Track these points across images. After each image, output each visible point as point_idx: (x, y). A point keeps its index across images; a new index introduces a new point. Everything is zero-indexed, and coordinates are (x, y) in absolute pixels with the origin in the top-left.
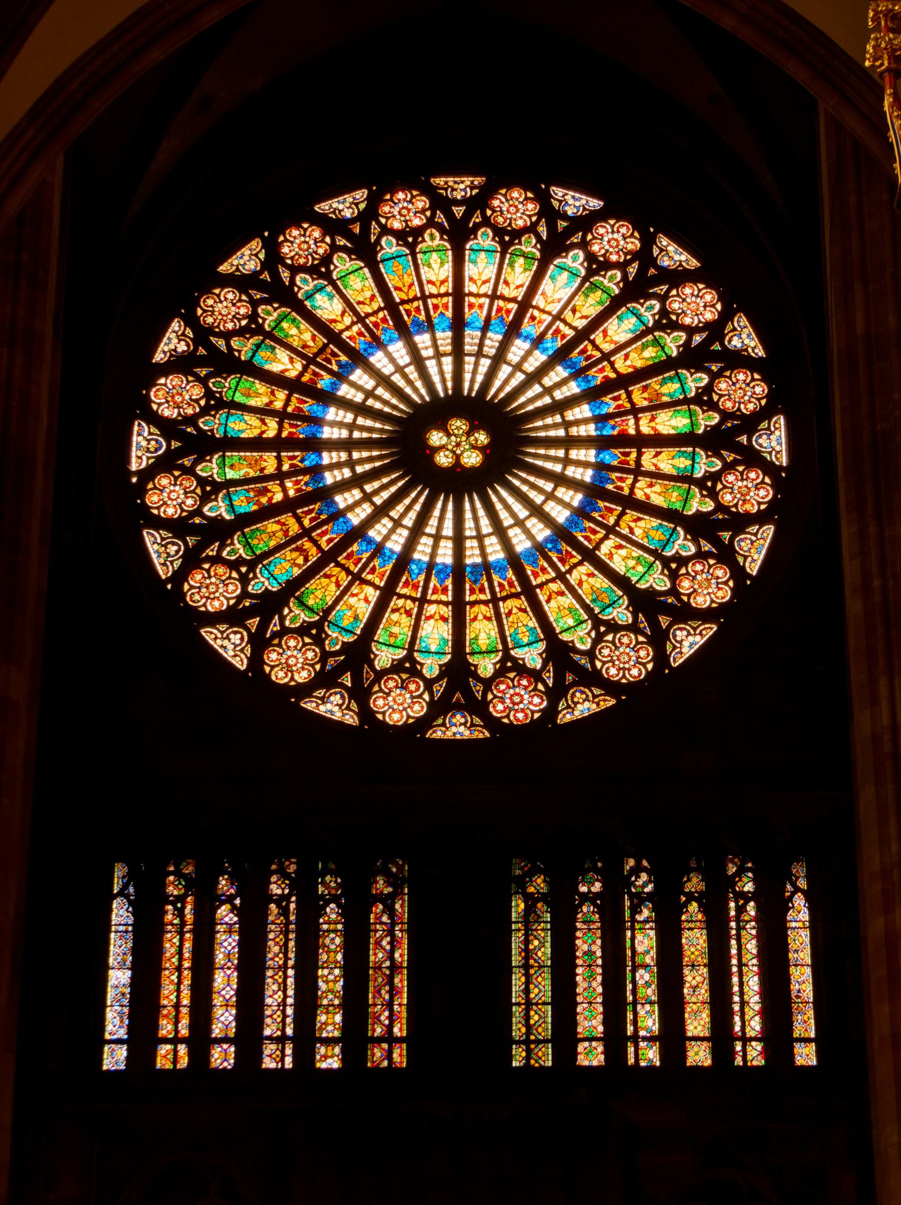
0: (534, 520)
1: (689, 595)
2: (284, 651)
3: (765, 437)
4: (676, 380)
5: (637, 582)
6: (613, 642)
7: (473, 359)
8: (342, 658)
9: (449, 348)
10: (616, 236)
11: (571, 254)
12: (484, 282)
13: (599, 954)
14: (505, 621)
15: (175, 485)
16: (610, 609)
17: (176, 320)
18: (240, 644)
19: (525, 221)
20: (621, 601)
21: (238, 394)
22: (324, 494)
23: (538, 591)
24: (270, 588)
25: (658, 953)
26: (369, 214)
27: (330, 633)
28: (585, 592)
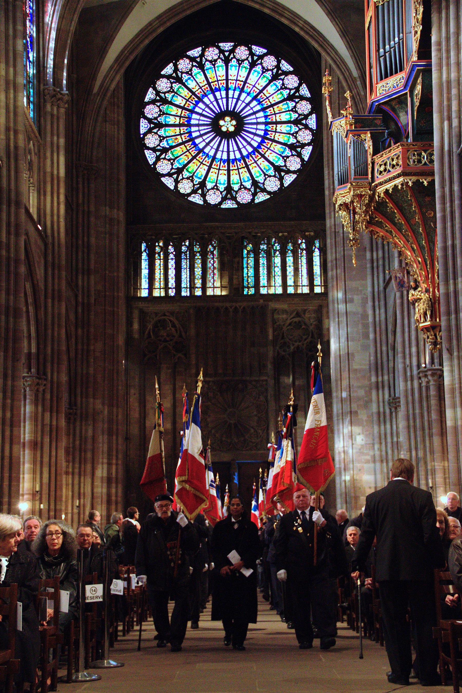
13: (266, 263)
22: (192, 140)
26: (202, 55)
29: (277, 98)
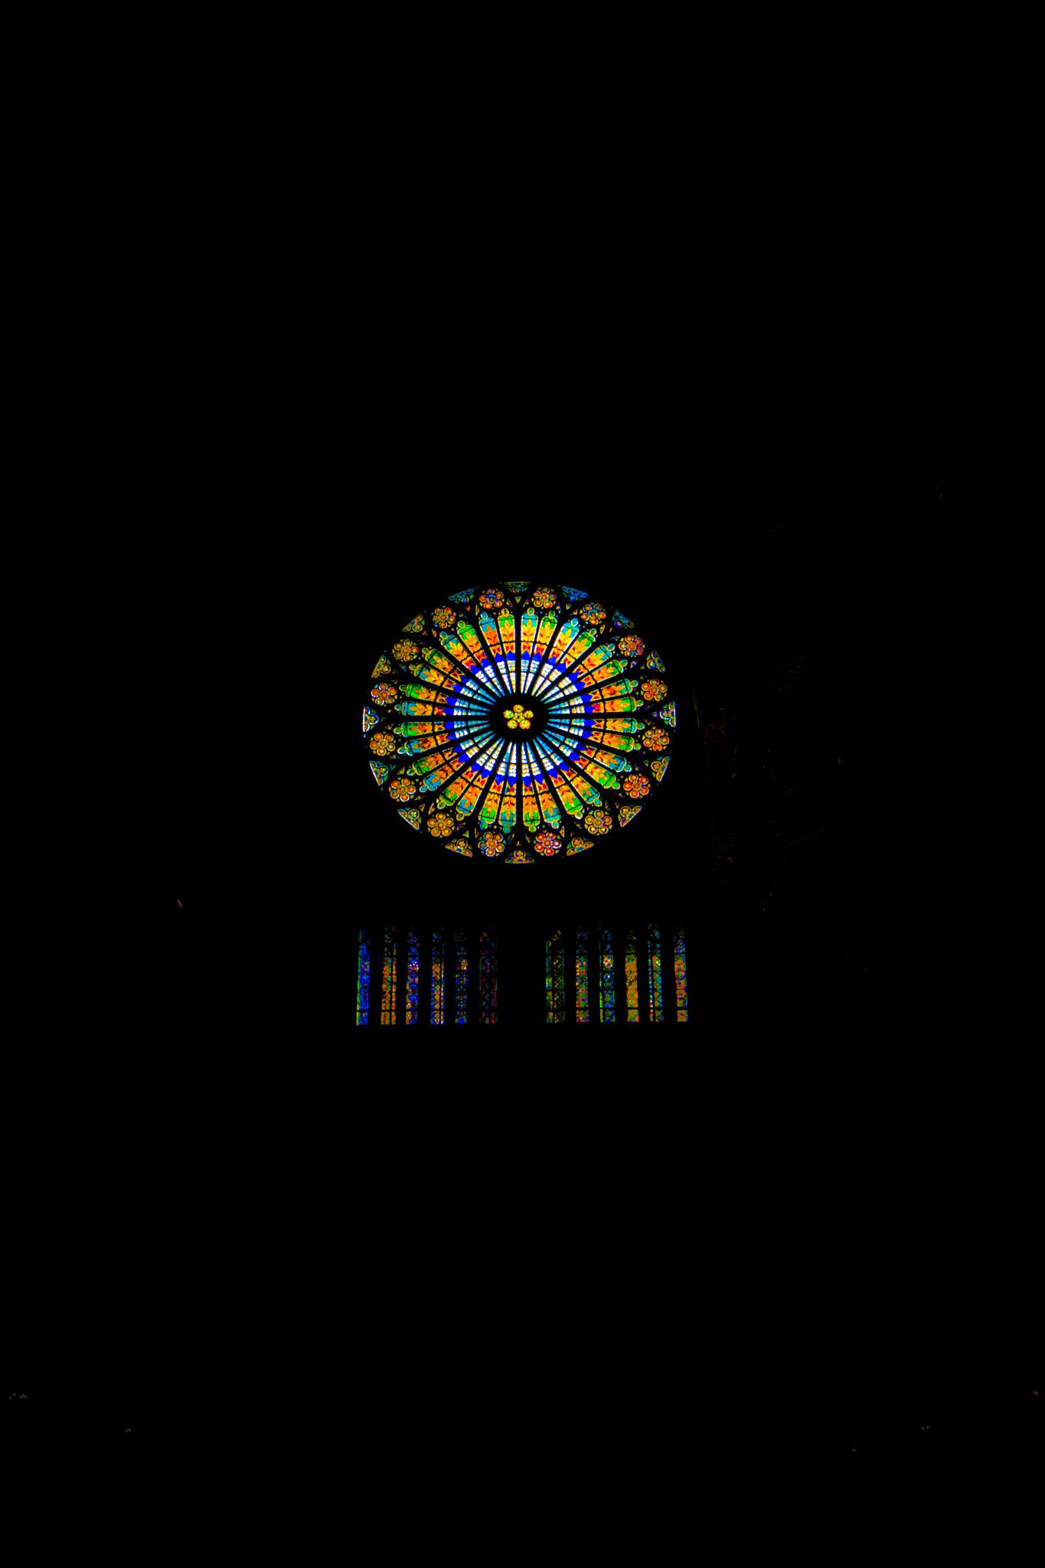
1: (629, 792)
6: (593, 815)
12: (531, 635)
22: (455, 744)
23: (557, 790)
26: (475, 602)
29: (609, 672)
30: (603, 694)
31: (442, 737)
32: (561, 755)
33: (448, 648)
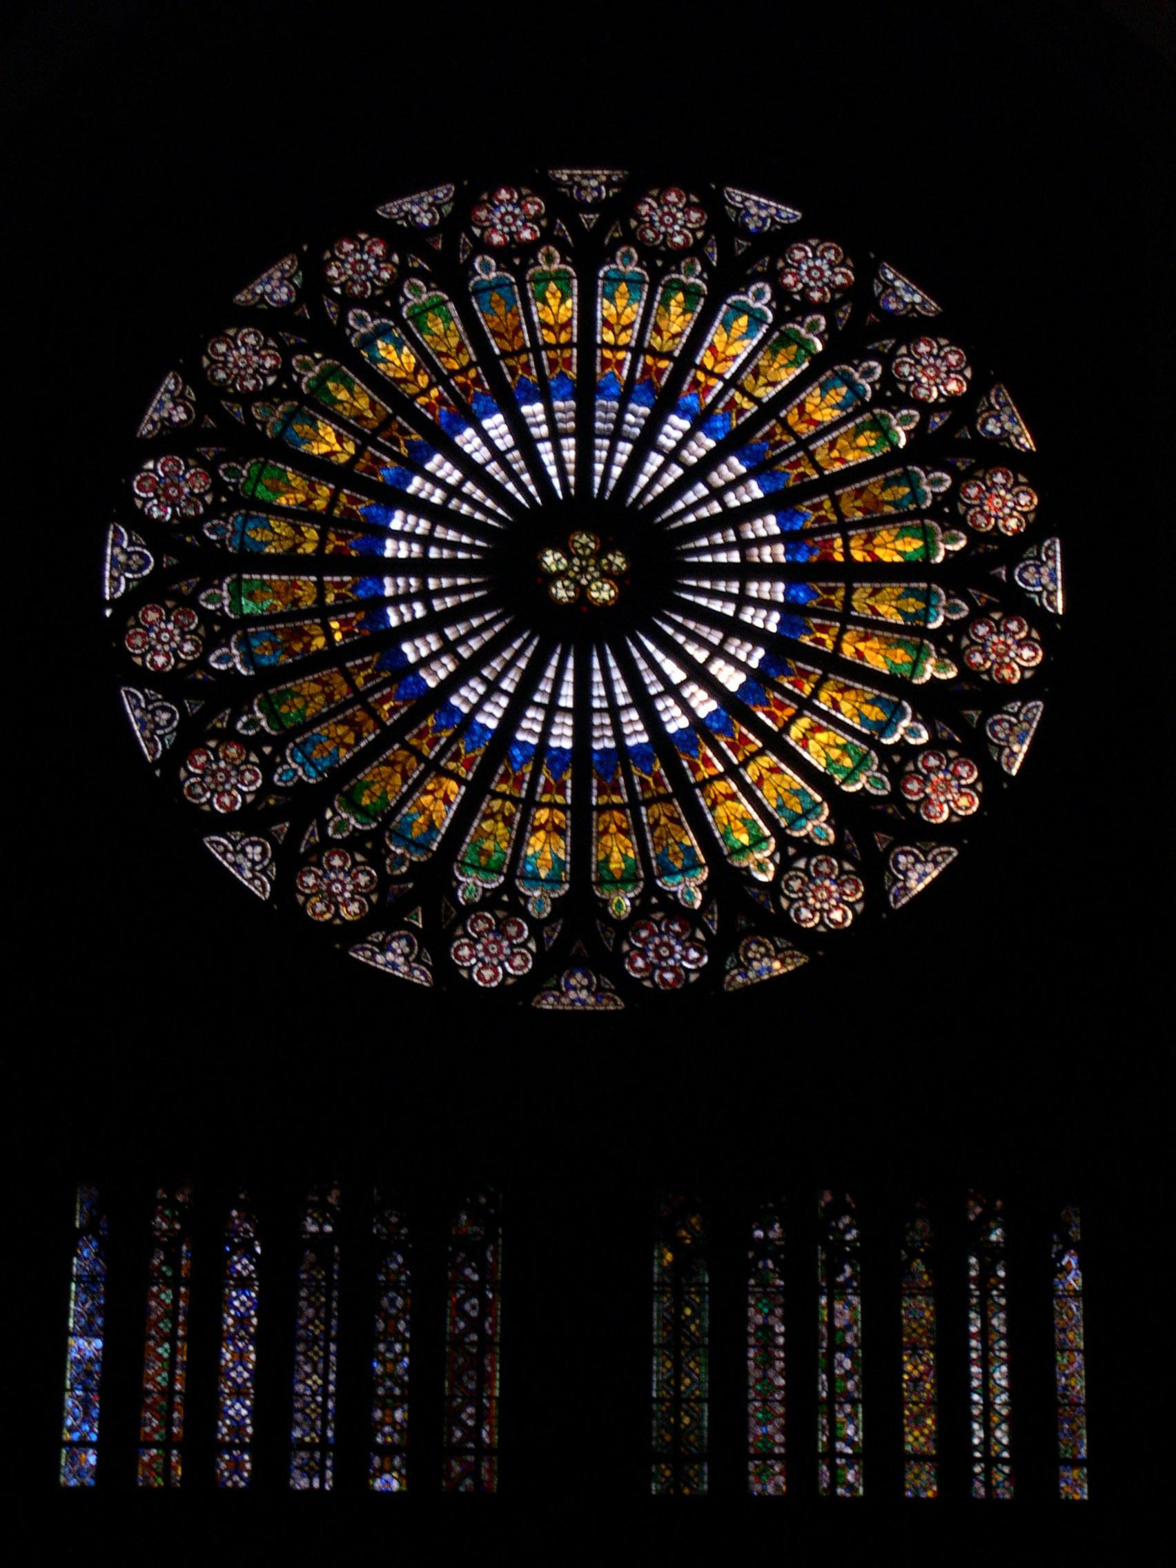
0: (693, 688)
1: (917, 804)
2: (324, 871)
3: (1032, 569)
4: (904, 481)
5: (844, 782)
7: (606, 443)
8: (410, 885)
9: (572, 425)
10: (818, 263)
11: (753, 288)
13: (780, 1328)
14: (649, 836)
15: (167, 621)
16: (803, 822)
17: (171, 374)
18: (261, 862)
19: (686, 237)
20: (819, 810)
21: (260, 488)
23: (698, 792)
24: (305, 778)
25: (863, 1330)
27: (393, 848)
28: (768, 796)
30: (844, 510)
31: (343, 623)
32: (714, 687)
33: (376, 360)
